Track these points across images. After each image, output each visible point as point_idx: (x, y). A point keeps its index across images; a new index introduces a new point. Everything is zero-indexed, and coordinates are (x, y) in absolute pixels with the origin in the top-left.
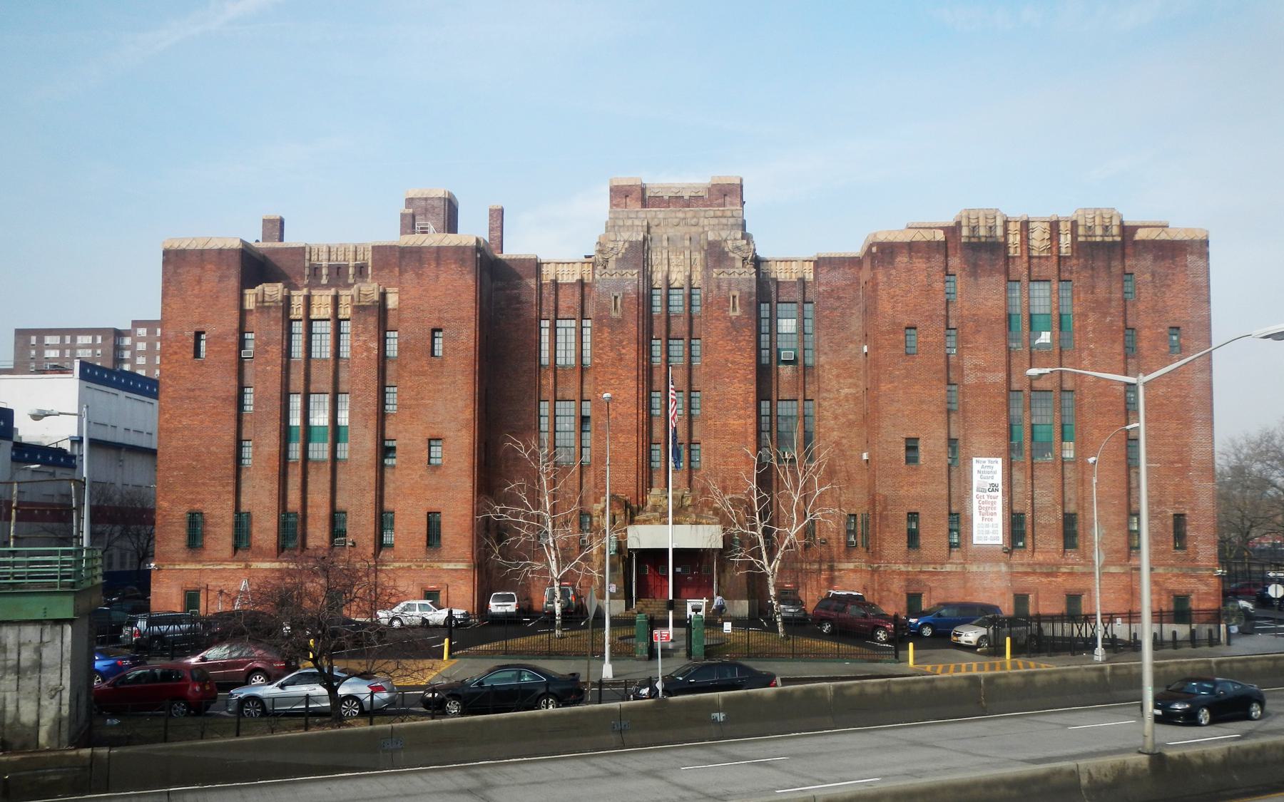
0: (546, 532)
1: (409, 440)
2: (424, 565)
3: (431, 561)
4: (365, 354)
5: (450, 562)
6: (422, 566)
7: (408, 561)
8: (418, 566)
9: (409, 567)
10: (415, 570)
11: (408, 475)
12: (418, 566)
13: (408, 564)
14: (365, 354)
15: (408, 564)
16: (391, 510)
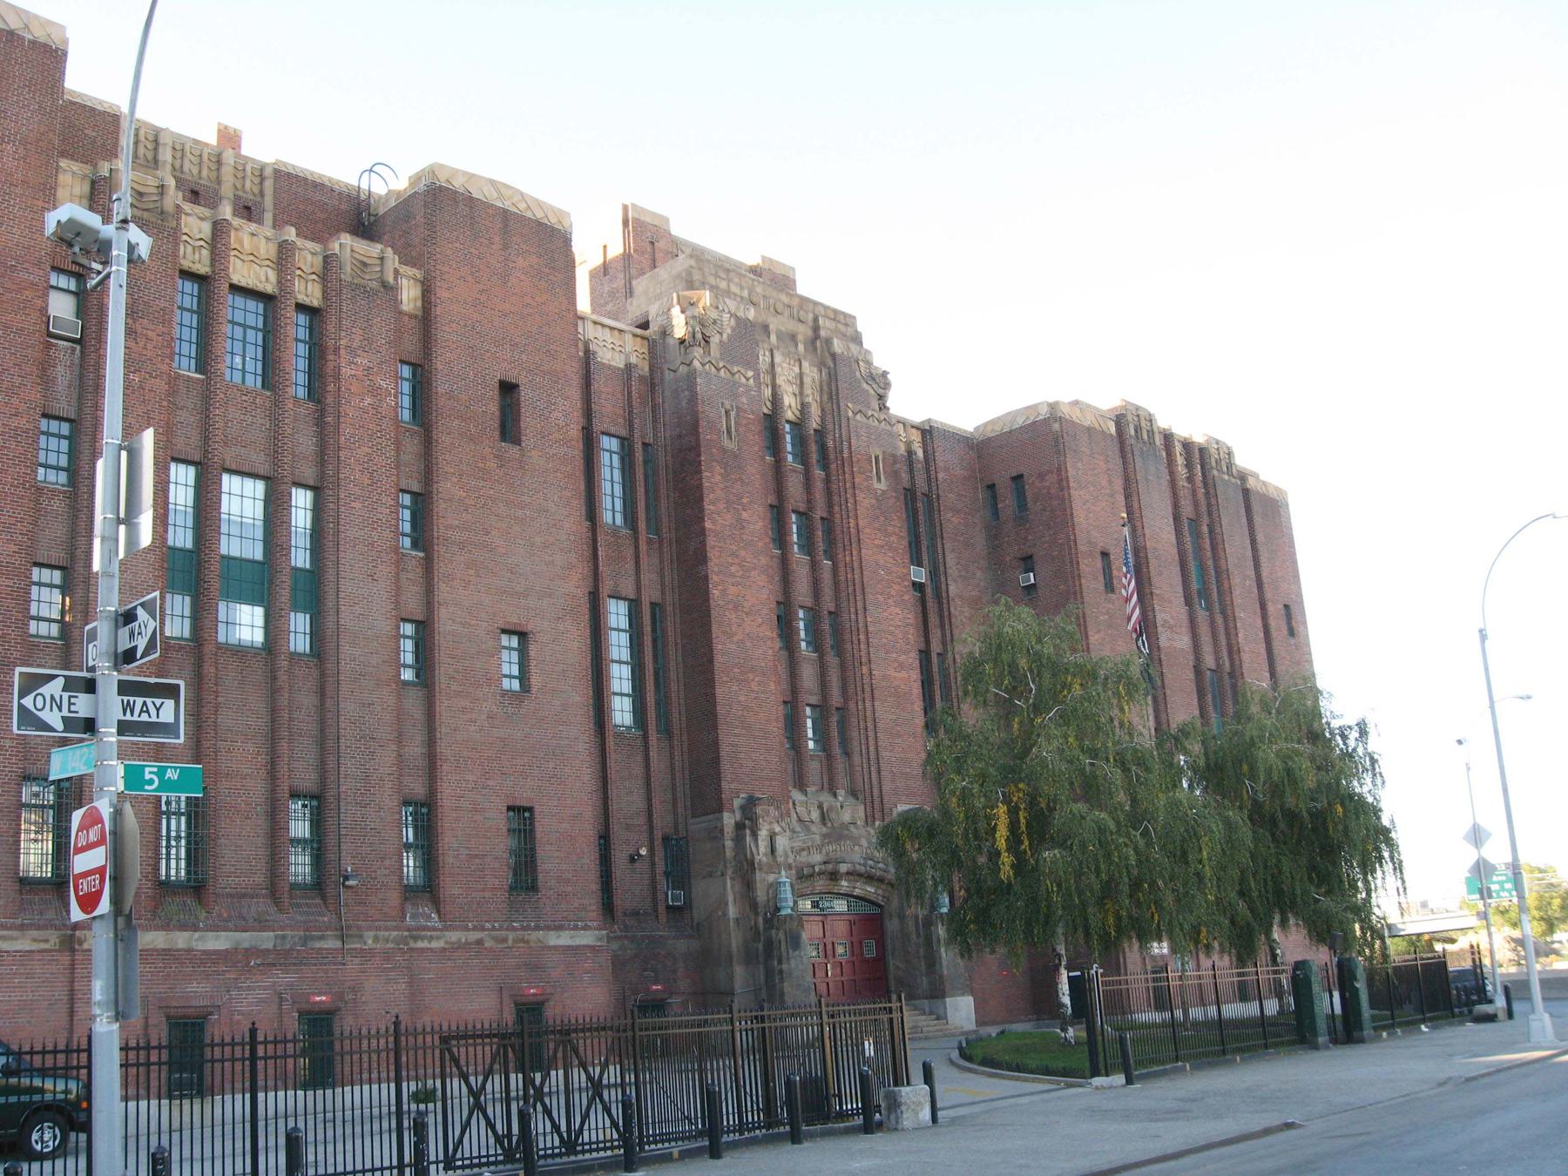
0: (1199, 876)
1: (463, 625)
2: (511, 936)
3: (523, 928)
4: (368, 400)
5: (560, 928)
6: (505, 940)
7: (475, 929)
8: (497, 940)
9: (480, 942)
10: (491, 950)
11: (463, 710)
12: (497, 940)
13: (477, 935)
14: (368, 400)
15: (477, 935)
16: (526, 804)
